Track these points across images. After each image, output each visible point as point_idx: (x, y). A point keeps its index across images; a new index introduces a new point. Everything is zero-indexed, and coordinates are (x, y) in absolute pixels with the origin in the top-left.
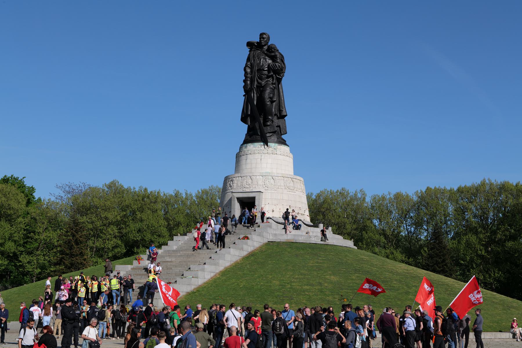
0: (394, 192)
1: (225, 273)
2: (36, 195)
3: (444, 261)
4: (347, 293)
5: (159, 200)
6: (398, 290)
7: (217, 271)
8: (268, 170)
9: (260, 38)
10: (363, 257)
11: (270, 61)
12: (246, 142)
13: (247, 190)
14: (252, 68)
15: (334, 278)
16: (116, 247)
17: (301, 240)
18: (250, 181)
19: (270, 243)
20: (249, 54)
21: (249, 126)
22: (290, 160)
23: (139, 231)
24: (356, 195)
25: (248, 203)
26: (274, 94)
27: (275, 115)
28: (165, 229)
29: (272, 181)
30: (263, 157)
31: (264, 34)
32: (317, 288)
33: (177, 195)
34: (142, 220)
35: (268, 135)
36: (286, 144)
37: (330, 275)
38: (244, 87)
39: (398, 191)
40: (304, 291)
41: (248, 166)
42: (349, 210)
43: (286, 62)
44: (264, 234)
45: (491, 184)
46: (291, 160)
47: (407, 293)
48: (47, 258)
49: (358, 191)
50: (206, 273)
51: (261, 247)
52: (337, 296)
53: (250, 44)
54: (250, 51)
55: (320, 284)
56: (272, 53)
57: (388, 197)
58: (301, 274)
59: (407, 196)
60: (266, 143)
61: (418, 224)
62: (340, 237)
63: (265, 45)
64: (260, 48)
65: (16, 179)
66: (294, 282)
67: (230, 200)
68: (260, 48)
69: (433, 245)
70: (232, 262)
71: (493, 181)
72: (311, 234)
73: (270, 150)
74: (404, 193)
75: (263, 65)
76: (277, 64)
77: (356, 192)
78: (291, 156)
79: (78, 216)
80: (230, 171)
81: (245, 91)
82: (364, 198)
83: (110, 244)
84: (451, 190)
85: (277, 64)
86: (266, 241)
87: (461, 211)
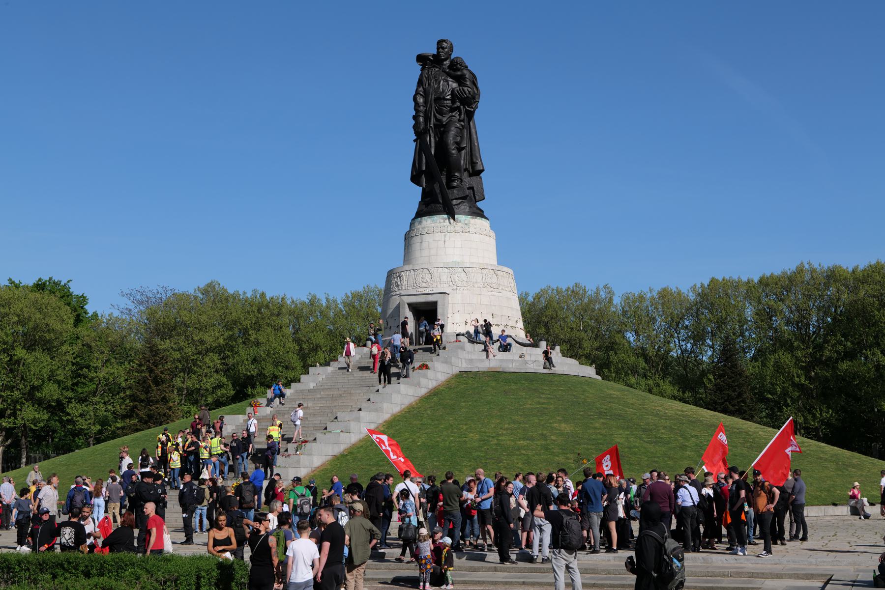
0: (657, 288)
2: (90, 309)
3: (740, 395)
4: (588, 449)
5: (284, 311)
6: (669, 443)
7: (381, 421)
8: (457, 259)
9: (438, 49)
11: (455, 85)
12: (420, 214)
13: (424, 291)
14: (426, 96)
15: (565, 427)
16: (219, 387)
17: (512, 367)
18: (428, 277)
20: (421, 75)
21: (424, 190)
23: (255, 360)
24: (597, 294)
25: (427, 312)
26: (462, 137)
27: (466, 170)
28: (295, 357)
29: (463, 275)
30: (447, 238)
31: (444, 41)
32: (539, 443)
33: (313, 302)
34: (258, 344)
35: (455, 202)
36: (483, 216)
37: (560, 422)
38: (415, 127)
39: (664, 286)
40: (519, 449)
41: (425, 253)
42: (586, 318)
43: (479, 85)
44: (454, 360)
45: (813, 271)
46: (493, 242)
47: (683, 448)
48: (109, 407)
49: (601, 287)
50: (362, 424)
51: (448, 381)
52: (572, 456)
53: (421, 59)
54: (422, 70)
55: (544, 437)
57: (649, 295)
58: (514, 422)
59: (679, 293)
60: (452, 214)
61: (698, 337)
62: (573, 362)
63: (446, 60)
64: (439, 64)
65: (56, 284)
66: (502, 435)
67: (398, 308)
68: (439, 64)
69: (723, 370)
70: (403, 406)
71: (816, 266)
72: (527, 358)
73: (458, 226)
74: (674, 289)
75: (443, 91)
76: (466, 89)
77: (597, 289)
78: (493, 234)
79: (157, 340)
80: (397, 261)
81: (416, 133)
82: (611, 299)
83: (209, 383)
84: (748, 282)
85: (466, 89)
86: (456, 371)
87: (766, 315)
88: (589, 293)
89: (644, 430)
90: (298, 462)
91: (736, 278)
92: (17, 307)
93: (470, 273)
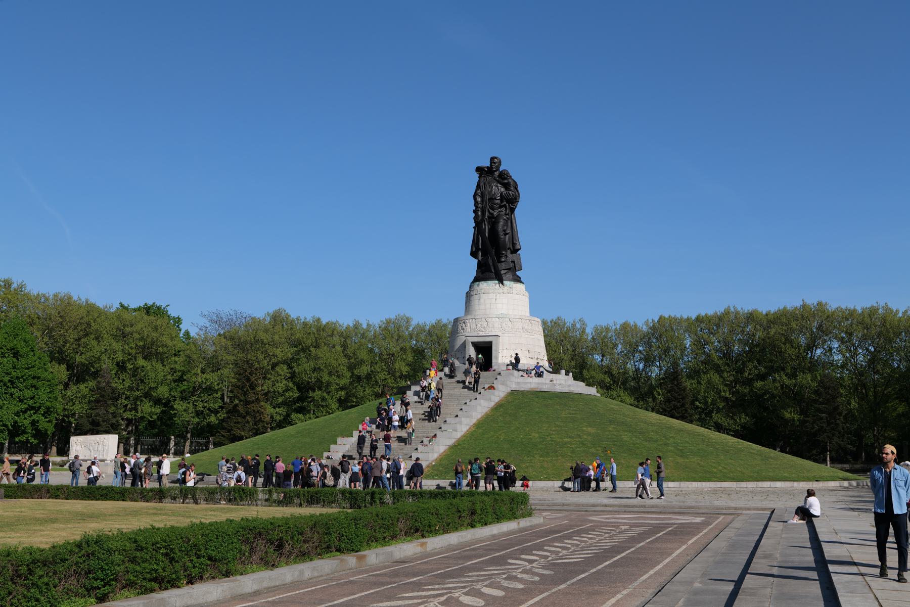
0: (620, 321)
1: (479, 425)
3: (683, 405)
5: (335, 333)
11: (503, 190)
12: (477, 279)
14: (482, 196)
15: (591, 430)
16: (287, 390)
17: (545, 388)
18: (485, 324)
19: (513, 392)
20: (479, 181)
21: (479, 262)
22: (526, 299)
23: (314, 370)
24: (574, 325)
25: (485, 349)
28: (345, 368)
29: (509, 323)
33: (357, 326)
34: (317, 358)
37: (587, 426)
39: (625, 321)
41: (482, 307)
42: (565, 342)
43: (519, 189)
44: (508, 383)
46: (527, 299)
47: (667, 445)
51: (506, 397)
53: (479, 169)
54: (480, 177)
56: (504, 179)
58: (558, 426)
59: (636, 326)
60: (501, 281)
61: (648, 360)
64: (491, 174)
65: (159, 308)
67: (464, 345)
68: (491, 174)
73: (505, 289)
74: (632, 323)
80: (460, 313)
81: (475, 222)
82: (584, 329)
83: (281, 386)
84: (688, 319)
86: (509, 390)
87: (700, 344)
89: (640, 433)
90: (433, 449)
91: (678, 316)
92: (138, 327)
93: (510, 320)
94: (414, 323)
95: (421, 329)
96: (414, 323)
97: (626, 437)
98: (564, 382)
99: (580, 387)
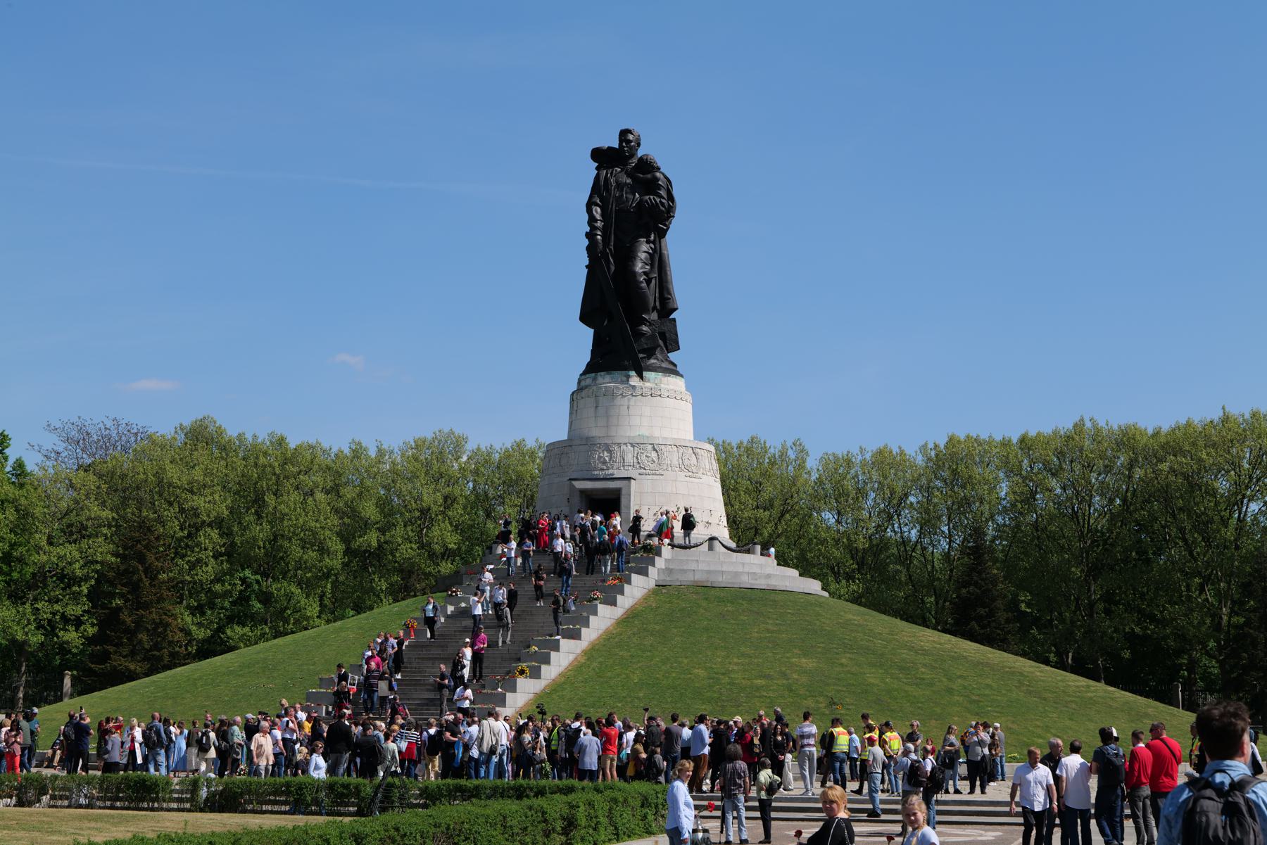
0: (872, 446)
4: (839, 691)
7: (579, 651)
10: (850, 616)
12: (593, 368)
15: (808, 663)
20: (597, 178)
24: (783, 454)
29: (654, 454)
30: (632, 403)
32: (779, 682)
33: (357, 452)
35: (641, 356)
36: (677, 373)
38: (591, 249)
43: (675, 193)
49: (789, 443)
51: (646, 598)
52: (821, 699)
53: (597, 154)
55: (784, 675)
56: (646, 176)
57: (860, 457)
58: (743, 655)
59: (902, 453)
61: (927, 524)
71: (1102, 424)
74: (895, 450)
77: (783, 447)
84: (1005, 444)
88: (772, 450)
89: (901, 669)
91: (984, 436)
94: (470, 446)
95: (482, 460)
96: (470, 446)
97: (873, 677)
98: (762, 570)
99: (789, 579)
